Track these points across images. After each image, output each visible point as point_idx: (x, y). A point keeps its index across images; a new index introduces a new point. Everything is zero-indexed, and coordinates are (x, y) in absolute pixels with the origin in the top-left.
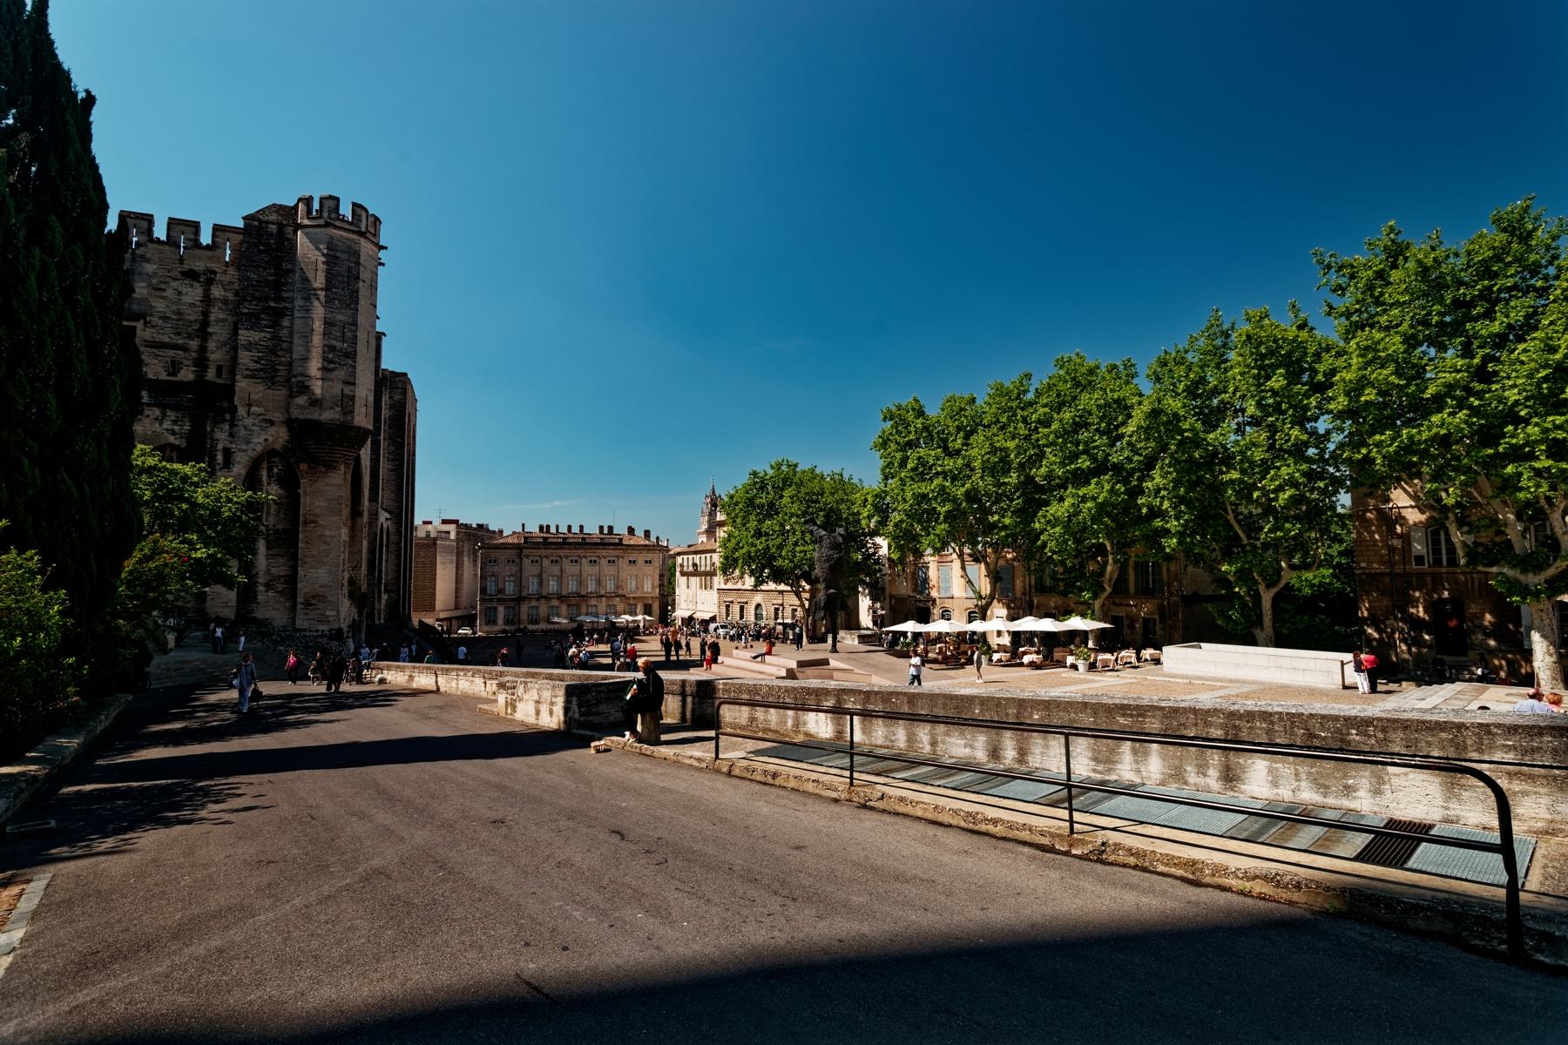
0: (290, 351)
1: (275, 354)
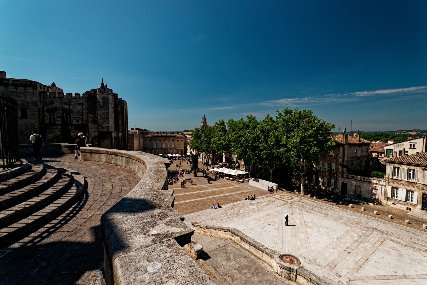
0: (97, 118)
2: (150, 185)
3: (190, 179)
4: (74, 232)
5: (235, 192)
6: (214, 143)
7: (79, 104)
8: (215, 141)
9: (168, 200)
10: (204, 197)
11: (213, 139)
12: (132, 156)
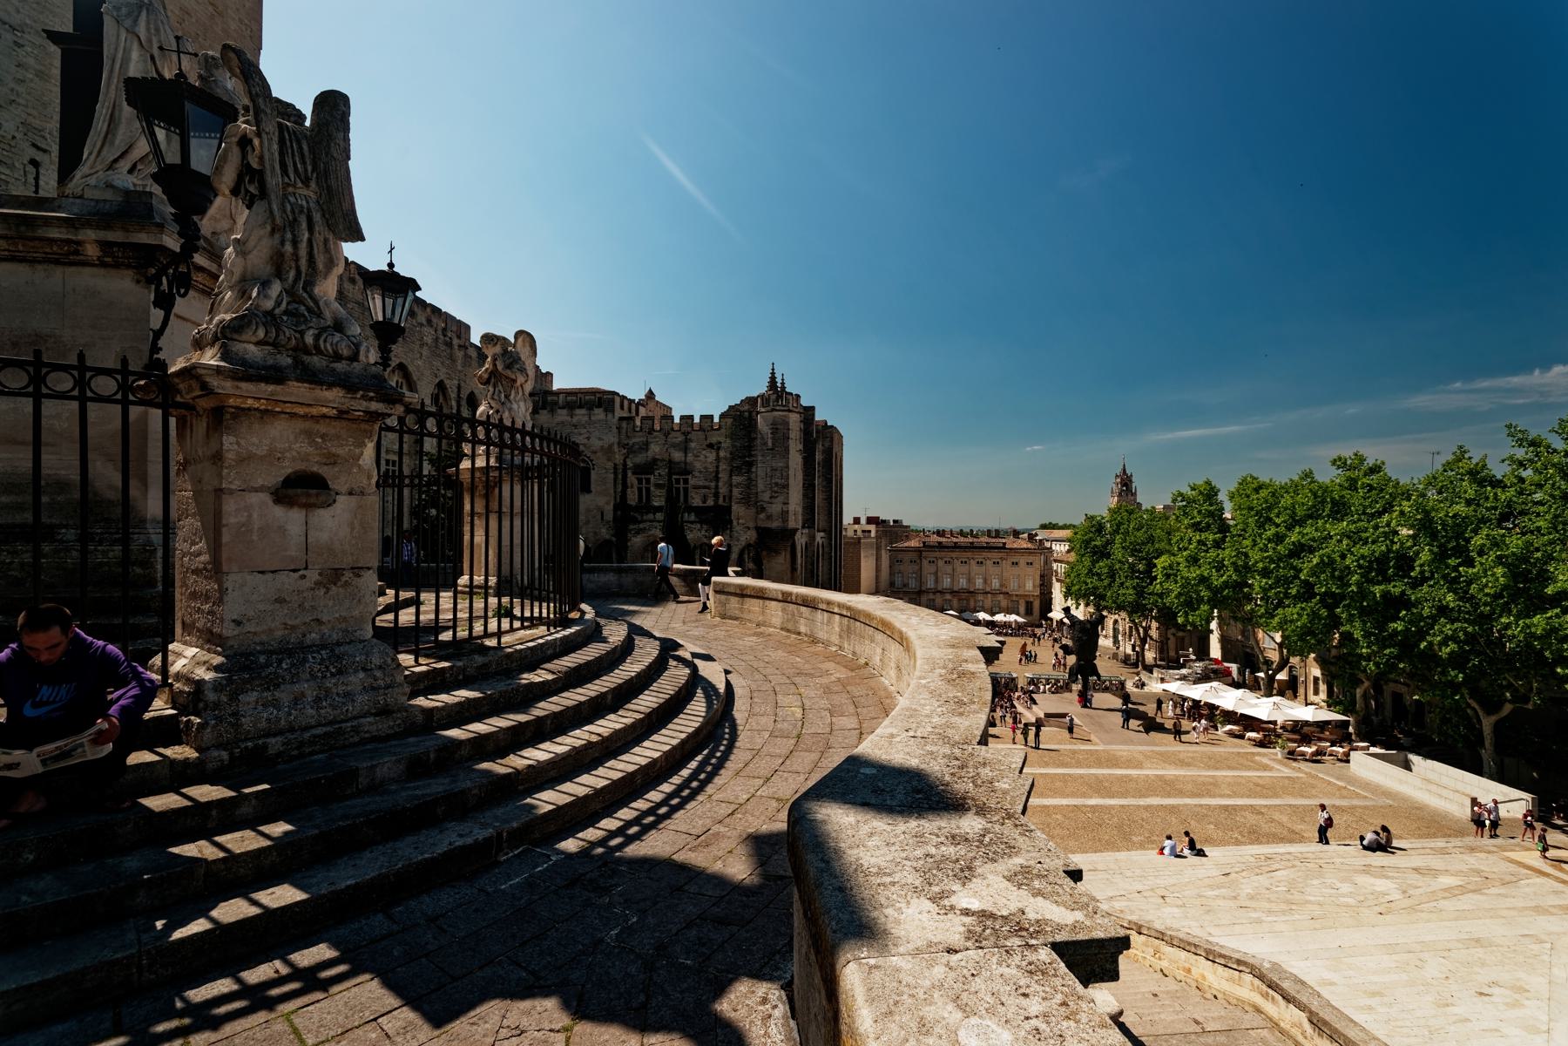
0: (756, 486)
1: (749, 488)
2: (936, 720)
3: (1064, 716)
4: (702, 839)
5: (1276, 796)
6: (1168, 576)
7: (711, 446)
8: (1171, 566)
9: (1006, 786)
10: (1124, 795)
11: (1162, 562)
12: (864, 611)
